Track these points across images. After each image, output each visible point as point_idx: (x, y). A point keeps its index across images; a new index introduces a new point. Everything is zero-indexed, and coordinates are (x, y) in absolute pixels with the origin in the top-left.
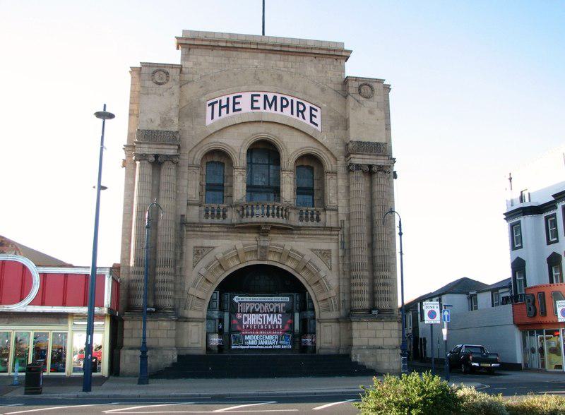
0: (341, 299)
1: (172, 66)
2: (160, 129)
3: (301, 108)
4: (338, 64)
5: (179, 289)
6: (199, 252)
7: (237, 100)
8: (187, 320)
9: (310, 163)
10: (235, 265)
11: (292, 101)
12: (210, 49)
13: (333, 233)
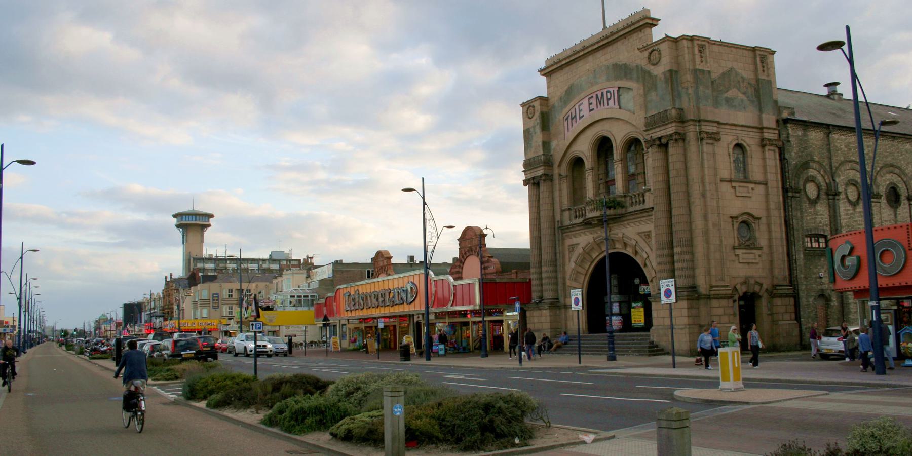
6: (572, 247)
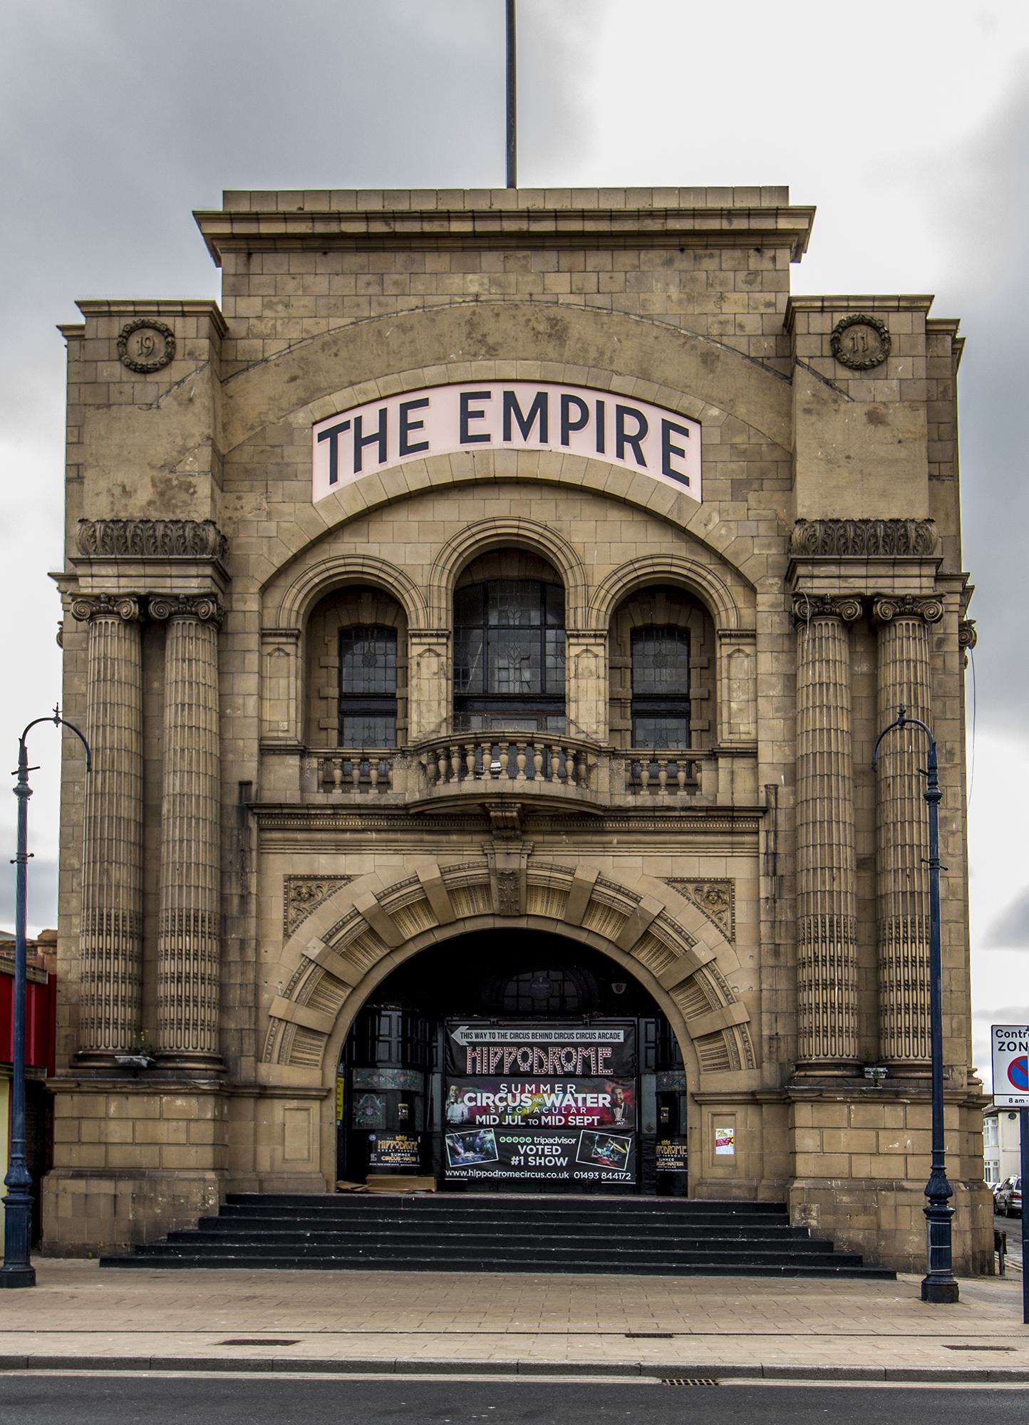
0: (766, 1032)
1: (184, 310)
2: (154, 515)
3: (631, 427)
4: (766, 264)
5: (231, 986)
7: (413, 416)
8: (264, 1093)
10: (417, 931)
11: (600, 405)
12: (315, 250)
13: (740, 826)
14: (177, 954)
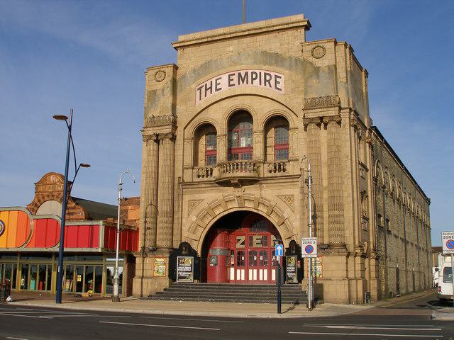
3: (268, 78)
9: (277, 122)
10: (220, 212)
14: (163, 222)
